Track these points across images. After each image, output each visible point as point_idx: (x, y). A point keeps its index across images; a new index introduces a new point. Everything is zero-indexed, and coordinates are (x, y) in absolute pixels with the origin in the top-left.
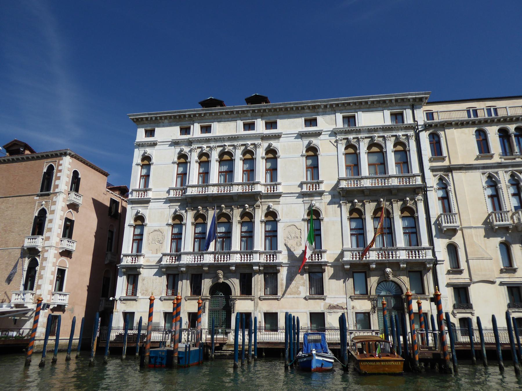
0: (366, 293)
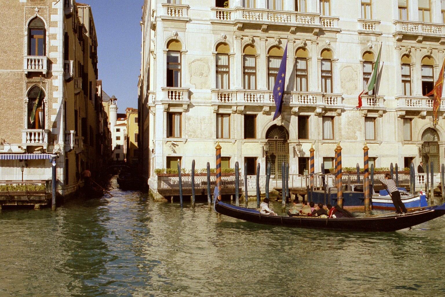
0: (373, 139)
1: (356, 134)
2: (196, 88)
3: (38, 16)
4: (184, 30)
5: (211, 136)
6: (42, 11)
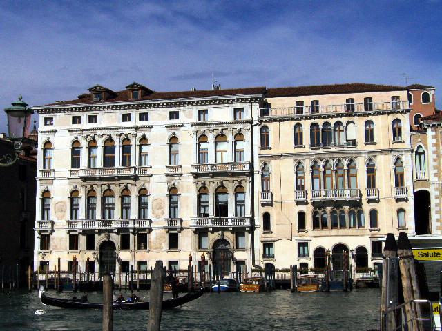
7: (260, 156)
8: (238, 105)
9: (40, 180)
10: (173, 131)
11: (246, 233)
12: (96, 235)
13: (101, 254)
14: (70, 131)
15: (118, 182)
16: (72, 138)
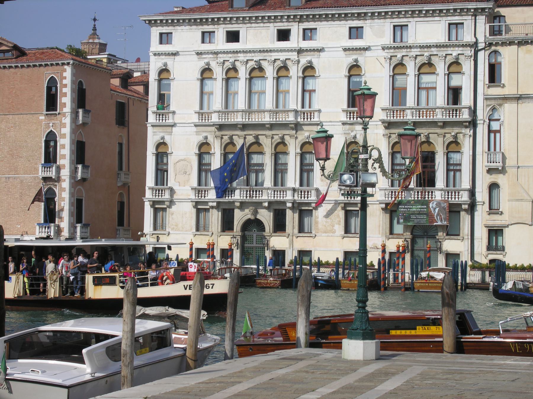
1: (334, 228)
2: (180, 186)
3: (53, 130)
4: (171, 133)
5: (191, 229)
6: (55, 126)
7: (487, 99)
8: (456, 19)
9: (153, 126)
10: (355, 57)
11: (463, 214)
12: (237, 211)
13: (244, 238)
14: (198, 54)
15: (269, 133)
16: (201, 64)
